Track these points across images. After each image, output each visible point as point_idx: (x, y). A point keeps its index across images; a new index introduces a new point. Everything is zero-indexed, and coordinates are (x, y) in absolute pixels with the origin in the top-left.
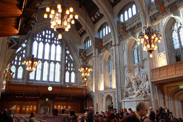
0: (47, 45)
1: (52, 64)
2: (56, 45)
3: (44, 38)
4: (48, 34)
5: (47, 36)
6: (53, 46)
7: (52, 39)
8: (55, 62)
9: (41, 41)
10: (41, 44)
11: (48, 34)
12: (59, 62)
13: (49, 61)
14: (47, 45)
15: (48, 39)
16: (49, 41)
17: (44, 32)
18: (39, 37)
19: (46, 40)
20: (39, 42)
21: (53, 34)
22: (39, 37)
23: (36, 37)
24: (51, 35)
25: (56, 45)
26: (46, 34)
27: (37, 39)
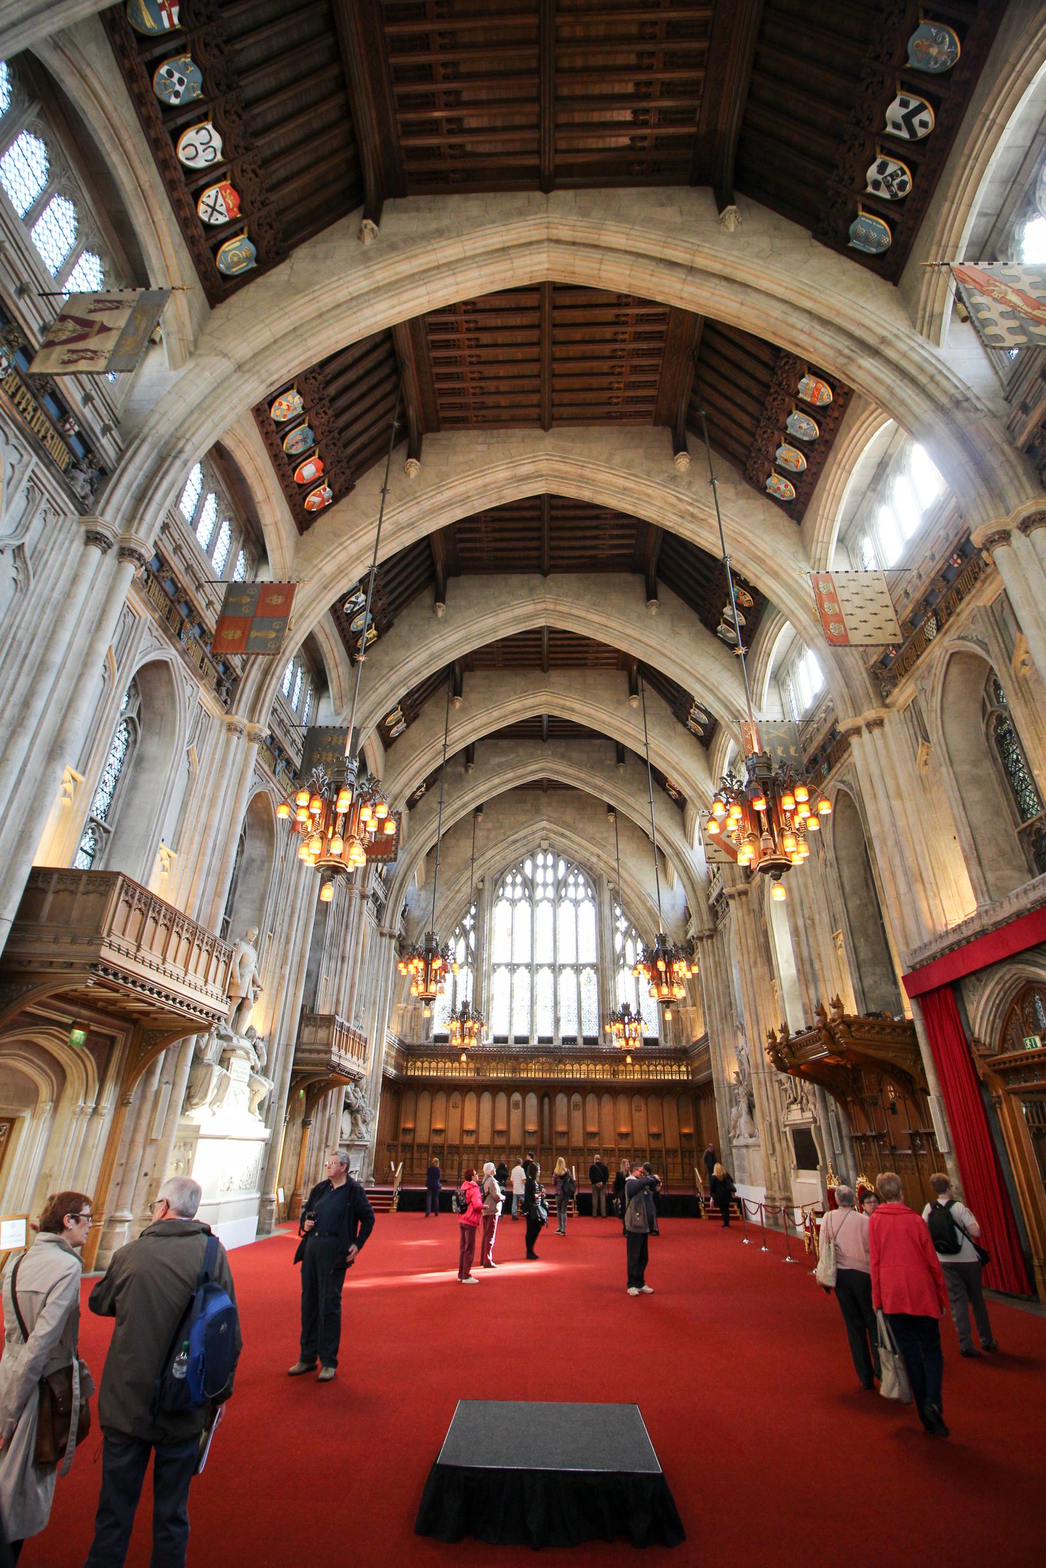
0: (544, 909)
1: (568, 974)
2: (576, 903)
3: (529, 884)
4: (545, 867)
5: (539, 878)
6: (566, 907)
7: (560, 884)
8: (578, 968)
9: (524, 897)
10: (524, 906)
11: (545, 867)
12: (593, 966)
13: (556, 969)
14: (544, 909)
15: (545, 885)
16: (550, 892)
17: (528, 865)
18: (514, 884)
19: (539, 893)
20: (513, 902)
21: (562, 865)
22: (514, 884)
23: (504, 885)
24: (555, 867)
25: (576, 903)
26: (535, 867)
27: (508, 891)
